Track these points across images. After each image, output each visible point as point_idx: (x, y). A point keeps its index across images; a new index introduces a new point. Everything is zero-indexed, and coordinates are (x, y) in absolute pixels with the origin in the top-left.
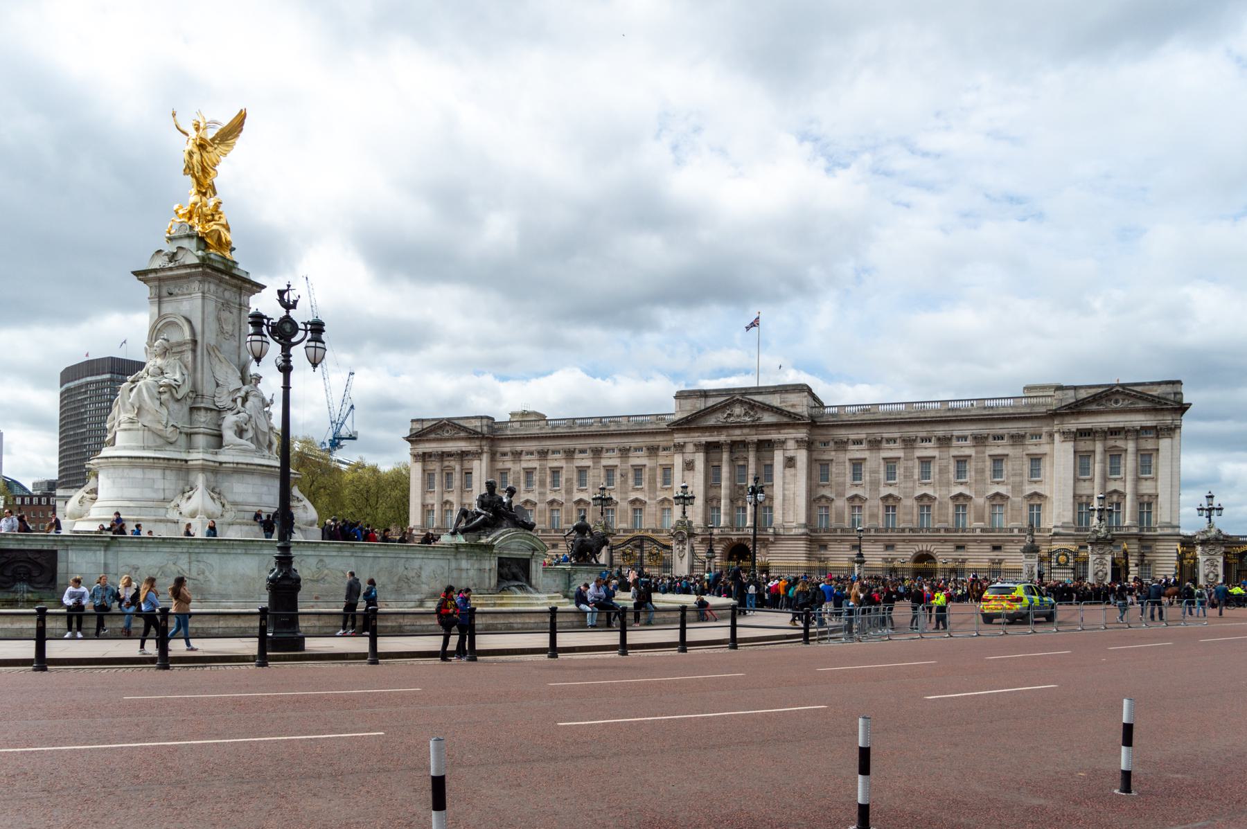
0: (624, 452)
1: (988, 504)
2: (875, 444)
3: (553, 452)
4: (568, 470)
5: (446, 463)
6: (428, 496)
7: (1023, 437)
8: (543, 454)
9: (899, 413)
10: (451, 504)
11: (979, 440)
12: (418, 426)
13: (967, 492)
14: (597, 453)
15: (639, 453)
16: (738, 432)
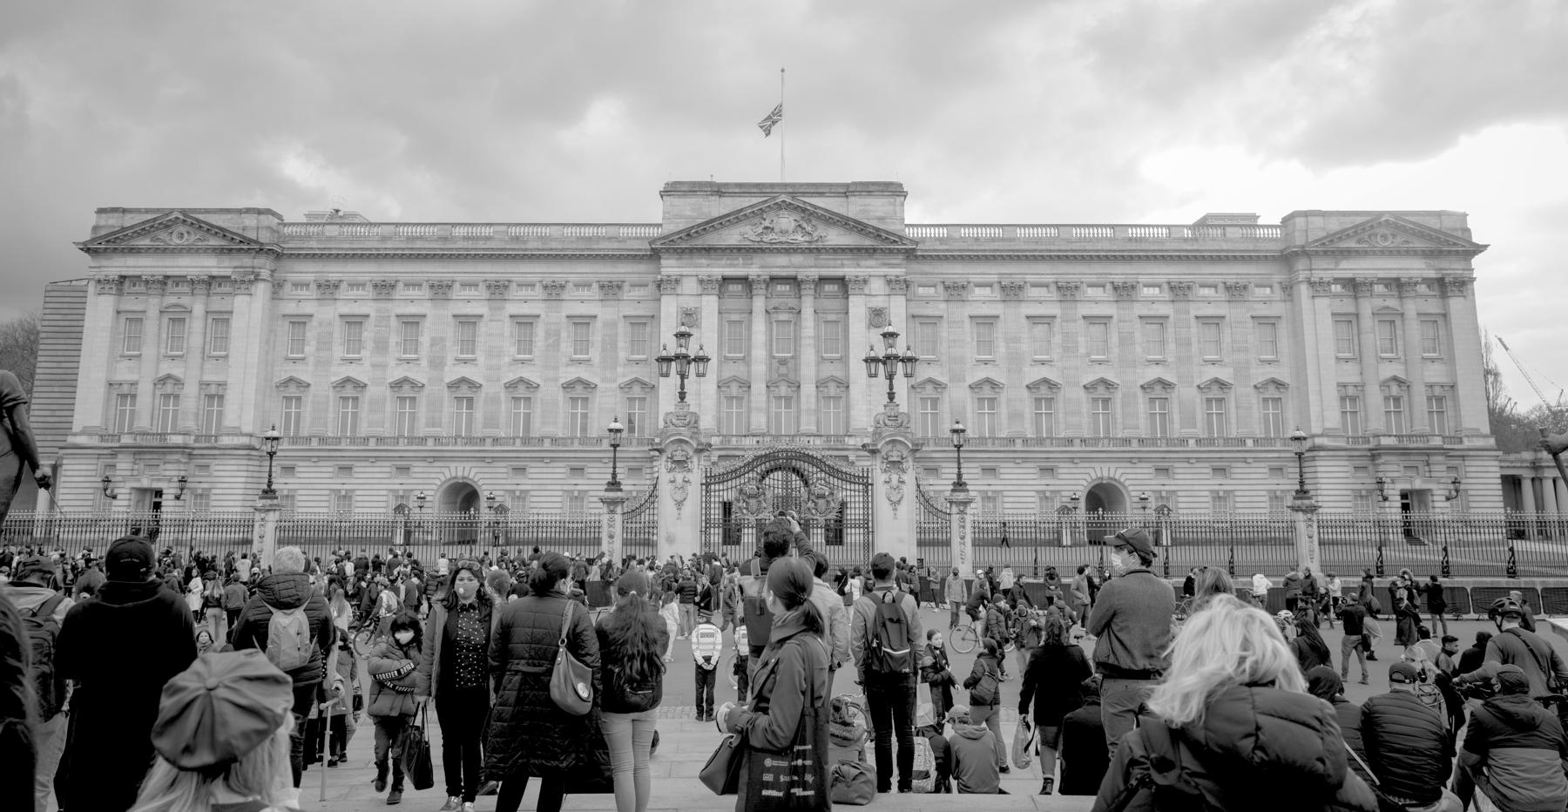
0: (554, 291)
1: (1198, 399)
2: (1012, 292)
3: (407, 285)
4: (438, 320)
5: (172, 300)
6: (124, 365)
7: (1245, 287)
8: (384, 289)
9: (1051, 240)
10: (178, 382)
11: (1179, 291)
12: (114, 222)
13: (1169, 378)
14: (498, 290)
15: (584, 293)
16: (782, 260)
